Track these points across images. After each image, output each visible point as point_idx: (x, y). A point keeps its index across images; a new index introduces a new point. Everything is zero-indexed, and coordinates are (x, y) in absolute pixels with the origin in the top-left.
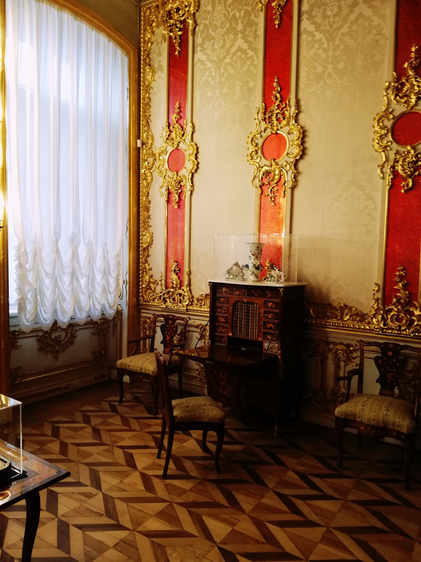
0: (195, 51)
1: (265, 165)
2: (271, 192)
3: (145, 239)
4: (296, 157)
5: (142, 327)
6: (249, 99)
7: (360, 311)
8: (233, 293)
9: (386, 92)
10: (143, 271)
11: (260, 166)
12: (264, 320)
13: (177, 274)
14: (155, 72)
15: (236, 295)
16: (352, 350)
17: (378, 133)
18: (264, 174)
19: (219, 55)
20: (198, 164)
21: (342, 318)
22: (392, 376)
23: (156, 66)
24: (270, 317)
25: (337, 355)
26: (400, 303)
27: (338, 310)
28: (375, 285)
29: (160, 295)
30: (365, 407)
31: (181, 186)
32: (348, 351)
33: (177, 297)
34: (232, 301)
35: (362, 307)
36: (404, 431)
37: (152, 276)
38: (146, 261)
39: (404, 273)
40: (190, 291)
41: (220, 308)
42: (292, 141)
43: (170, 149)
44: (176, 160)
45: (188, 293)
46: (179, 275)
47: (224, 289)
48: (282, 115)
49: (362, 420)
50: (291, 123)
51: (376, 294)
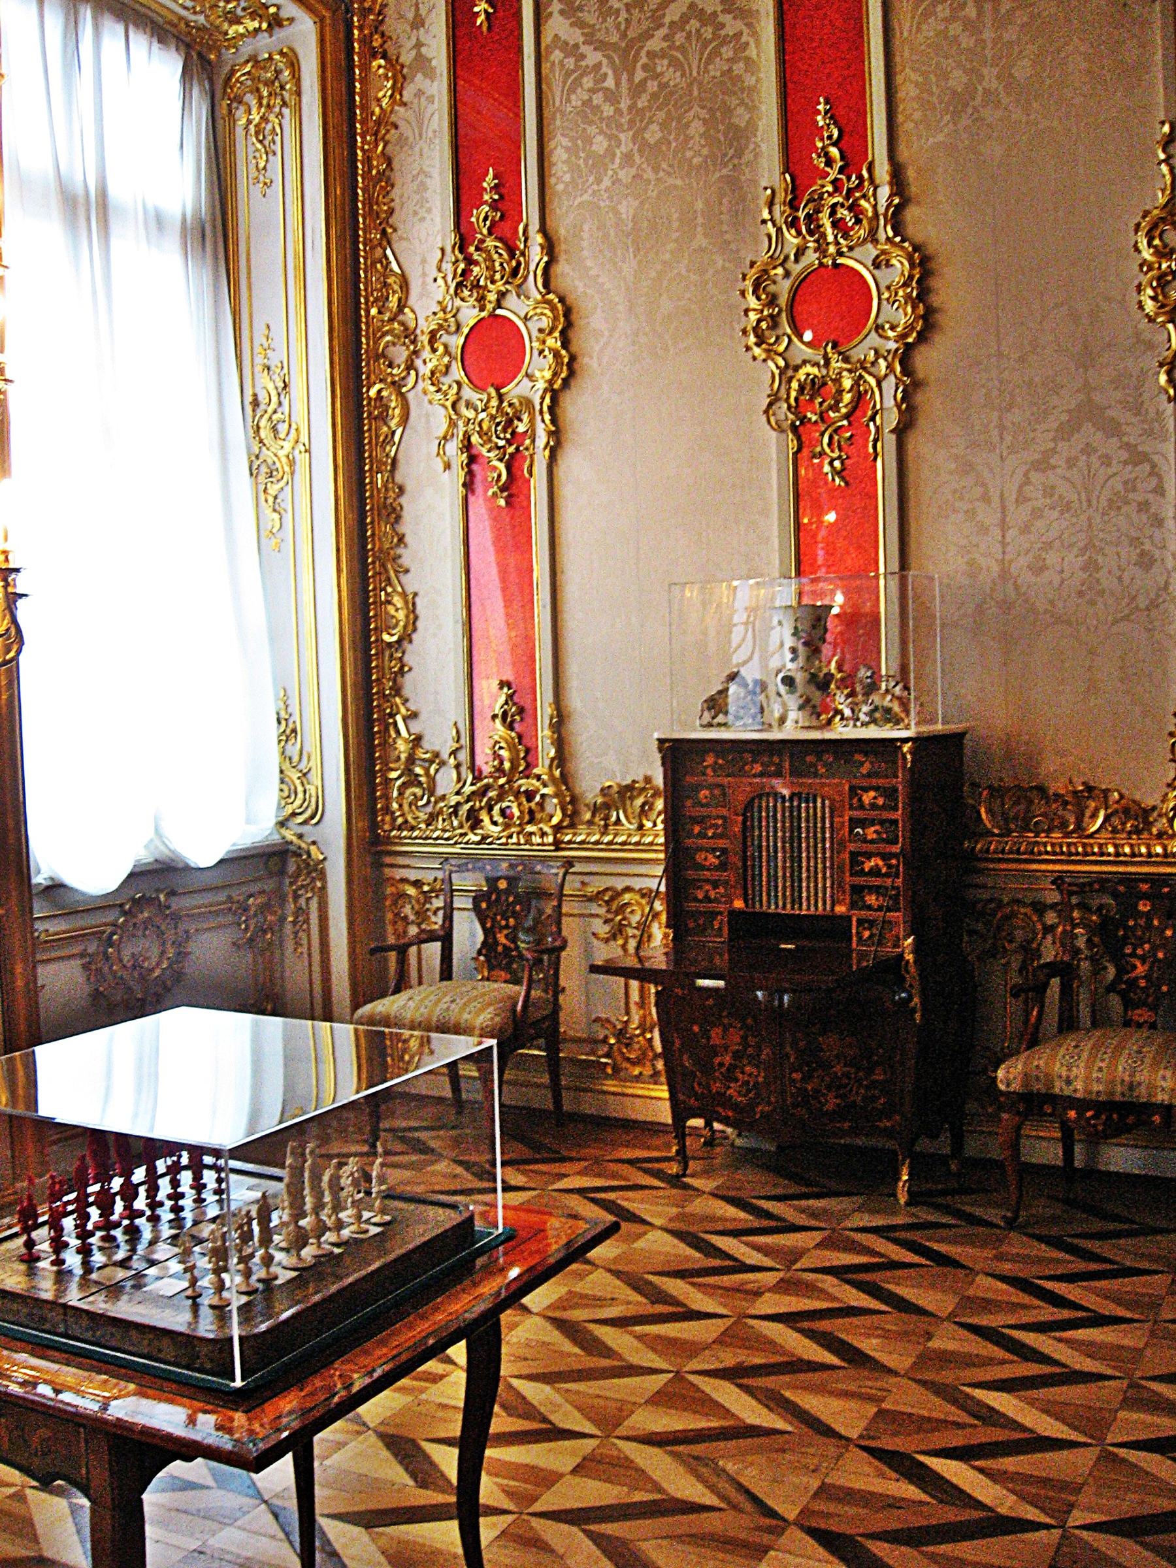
0: (544, 15)
1: (805, 362)
2: (830, 444)
4: (904, 336)
5: (389, 916)
6: (736, 161)
7: (1134, 801)
9: (1164, 151)
10: (387, 726)
11: (787, 366)
12: (852, 847)
14: (404, 77)
17: (1150, 269)
18: (802, 389)
19: (627, 28)
20: (573, 358)
21: (1079, 827)
23: (407, 57)
27: (1066, 803)
29: (454, 800)
31: (513, 433)
34: (740, 798)
38: (397, 690)
40: (565, 779)
41: (700, 820)
42: (888, 288)
43: (470, 315)
44: (491, 351)
47: (710, 760)
48: (850, 209)
50: (882, 236)
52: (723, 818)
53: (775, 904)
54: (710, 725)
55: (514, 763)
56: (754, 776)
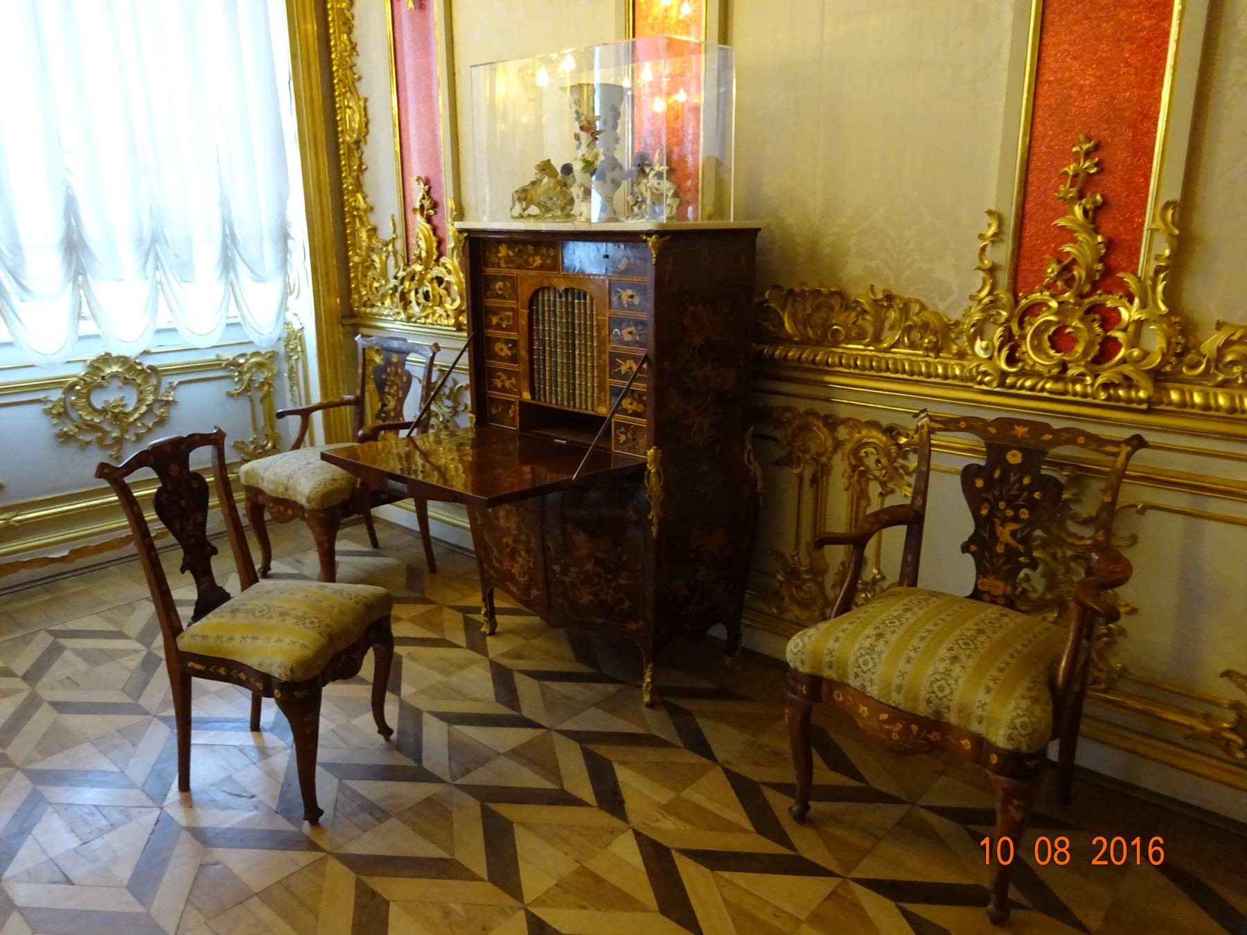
3: (350, 118)
7: (936, 314)
8: (526, 261)
12: (610, 347)
13: (429, 220)
15: (536, 269)
16: (907, 444)
21: (877, 339)
22: (1013, 534)
24: (628, 338)
25: (860, 460)
26: (1069, 282)
27: (864, 311)
28: (988, 219)
30: (881, 643)
32: (893, 449)
33: (433, 289)
34: (525, 292)
35: (943, 298)
36: (999, 738)
37: (374, 229)
38: (359, 187)
39: (1096, 165)
45: (458, 276)
46: (435, 220)
47: (503, 251)
49: (864, 687)
51: (988, 249)
52: (512, 309)
53: (555, 399)
54: (521, 216)
56: (536, 269)
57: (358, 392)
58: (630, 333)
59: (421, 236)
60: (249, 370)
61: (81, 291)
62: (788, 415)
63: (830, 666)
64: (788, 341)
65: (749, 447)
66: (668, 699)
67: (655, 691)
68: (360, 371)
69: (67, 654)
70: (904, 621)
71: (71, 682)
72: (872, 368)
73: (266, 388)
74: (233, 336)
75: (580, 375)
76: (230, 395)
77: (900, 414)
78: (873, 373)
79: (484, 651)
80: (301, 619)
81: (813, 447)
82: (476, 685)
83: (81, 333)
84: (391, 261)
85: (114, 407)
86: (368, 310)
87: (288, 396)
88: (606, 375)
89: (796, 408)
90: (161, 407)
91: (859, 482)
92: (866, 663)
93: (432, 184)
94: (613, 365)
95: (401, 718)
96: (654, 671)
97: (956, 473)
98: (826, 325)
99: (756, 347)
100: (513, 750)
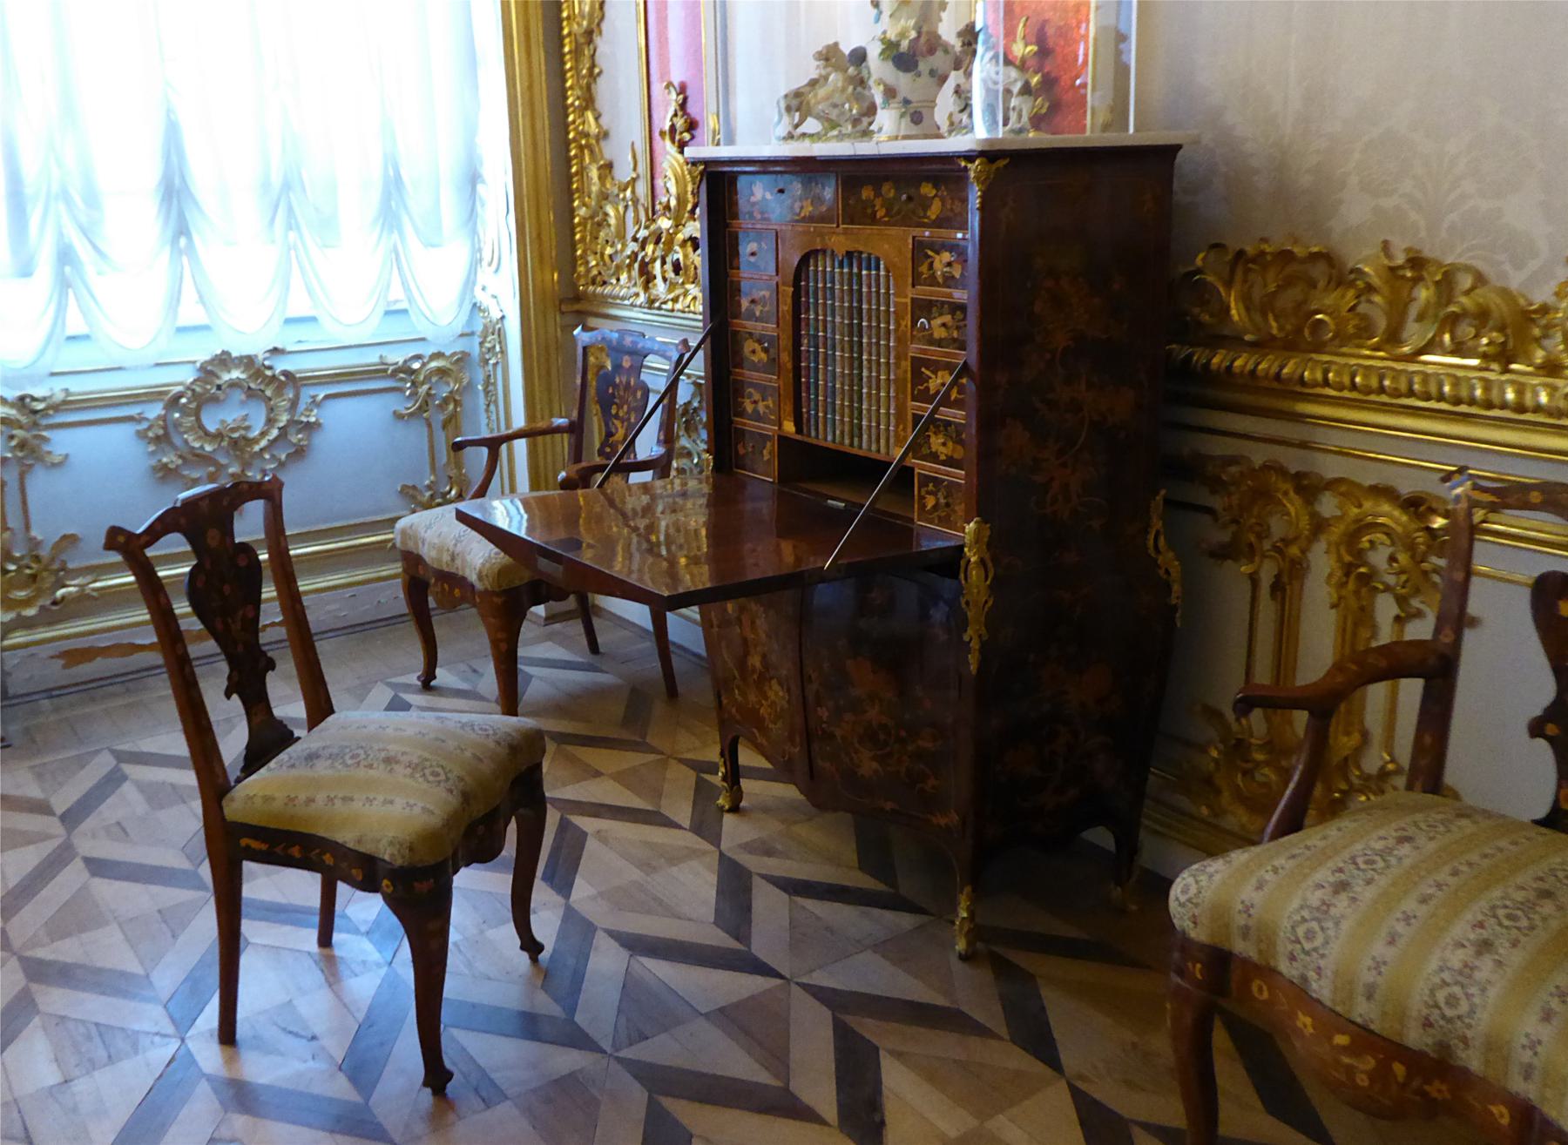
7: (1505, 293)
12: (914, 349)
21: (1393, 337)
25: (1359, 555)
27: (1370, 289)
30: (1342, 902)
32: (1421, 538)
33: (686, 256)
37: (609, 166)
38: (589, 101)
49: (1304, 978)
53: (830, 435)
54: (790, 136)
55: (681, 200)
57: (575, 414)
58: (944, 325)
59: (670, 173)
60: (427, 379)
61: (185, 259)
62: (1233, 469)
63: (1245, 932)
64: (1234, 341)
65: (1157, 524)
66: (995, 949)
67: (977, 933)
68: (579, 381)
69: (127, 787)
70: (1393, 861)
71: (120, 831)
72: (1382, 390)
73: (451, 407)
74: (397, 330)
75: (869, 394)
76: (398, 416)
77: (1415, 472)
78: (1384, 398)
79: (715, 839)
80: (416, 767)
81: (1277, 527)
82: (690, 893)
83: (181, 323)
84: (631, 214)
85: (233, 430)
86: (599, 290)
87: (484, 421)
88: (899, 393)
89: (1249, 459)
90: (299, 432)
91: (1357, 593)
92: (1310, 935)
93: (689, 92)
94: (918, 378)
95: (562, 935)
96: (976, 898)
97: (1527, 585)
98: (1303, 313)
99: (1179, 351)
100: (722, 1010)
